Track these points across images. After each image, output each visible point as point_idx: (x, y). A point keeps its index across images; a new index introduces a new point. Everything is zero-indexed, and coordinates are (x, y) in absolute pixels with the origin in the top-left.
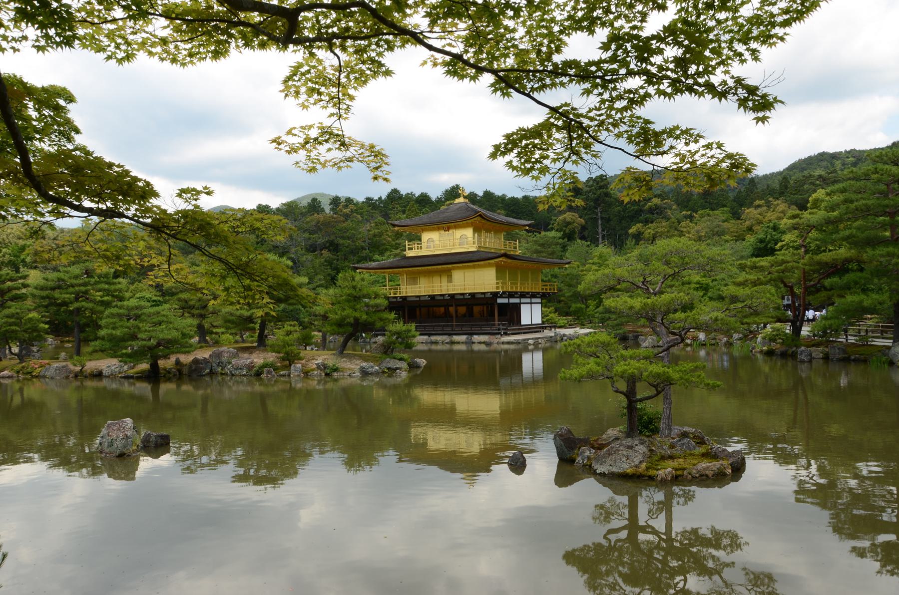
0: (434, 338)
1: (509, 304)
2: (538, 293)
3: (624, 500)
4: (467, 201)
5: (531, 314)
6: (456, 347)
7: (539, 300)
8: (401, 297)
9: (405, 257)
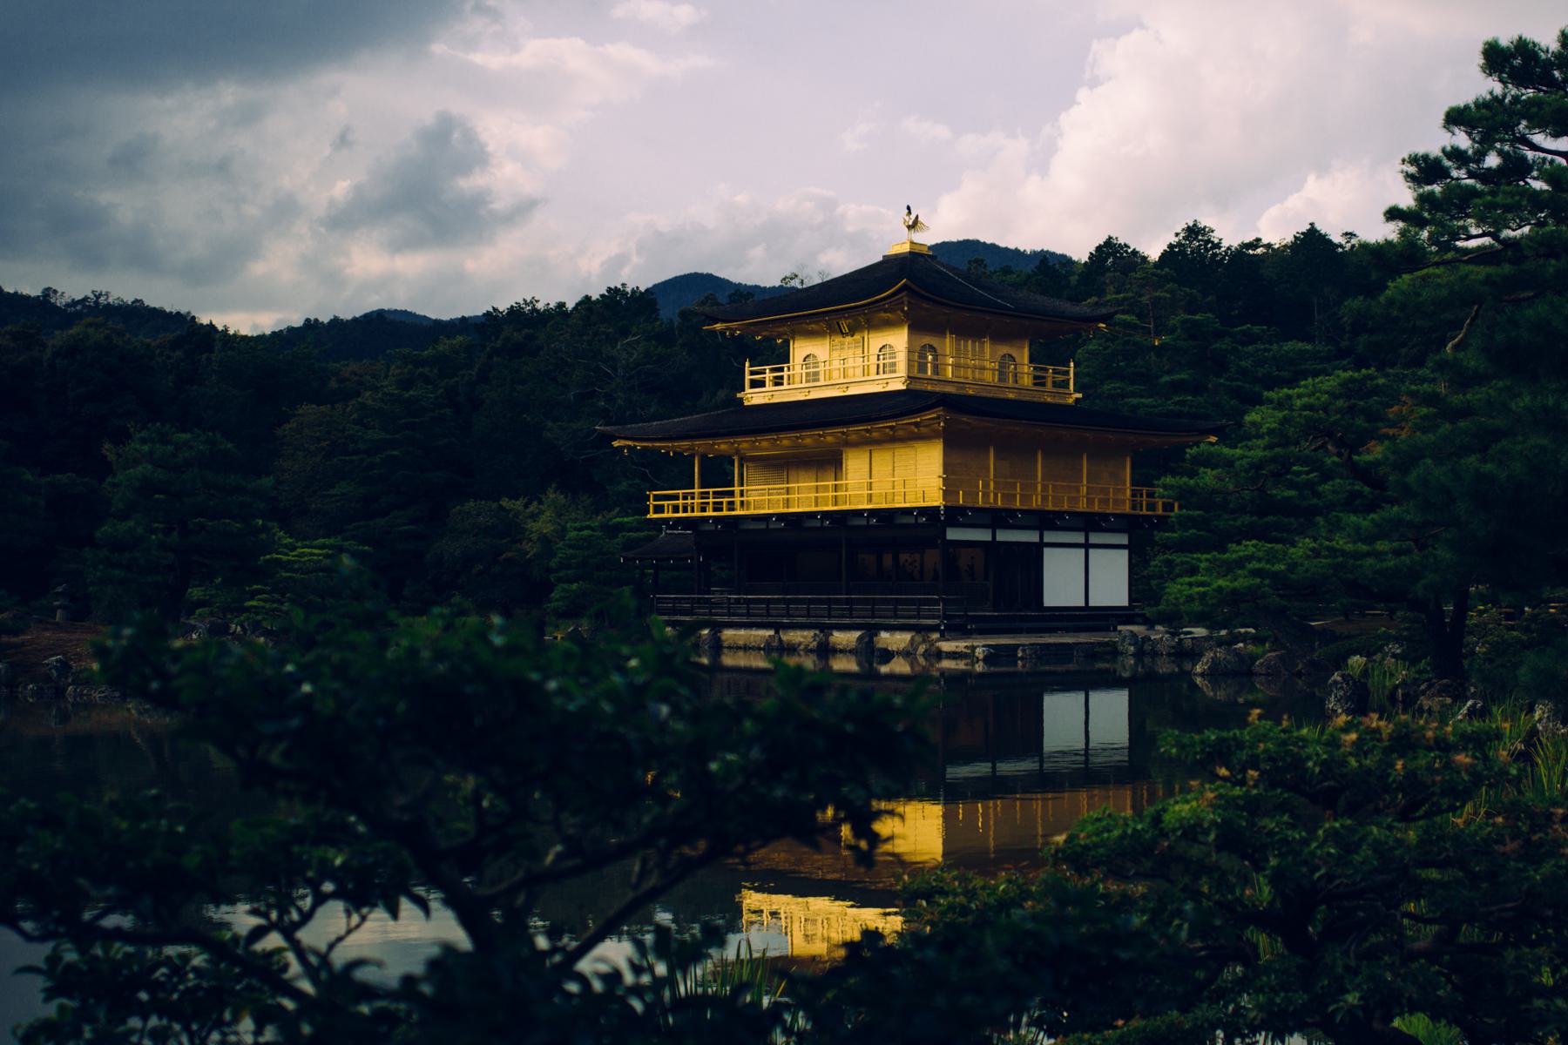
5: (1085, 578)
6: (843, 664)
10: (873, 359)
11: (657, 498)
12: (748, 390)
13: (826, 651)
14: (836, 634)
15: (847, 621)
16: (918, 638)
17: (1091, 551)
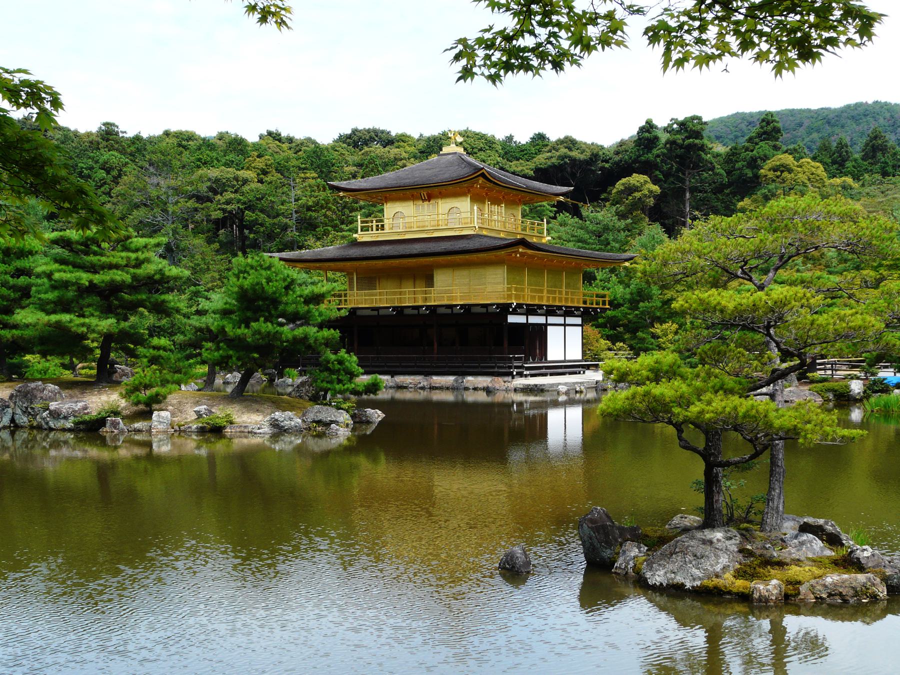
0: (400, 379)
1: (527, 325)
2: (577, 309)
3: (698, 638)
4: (460, 150)
5: (564, 342)
7: (578, 321)
9: (355, 243)
14: (435, 378)
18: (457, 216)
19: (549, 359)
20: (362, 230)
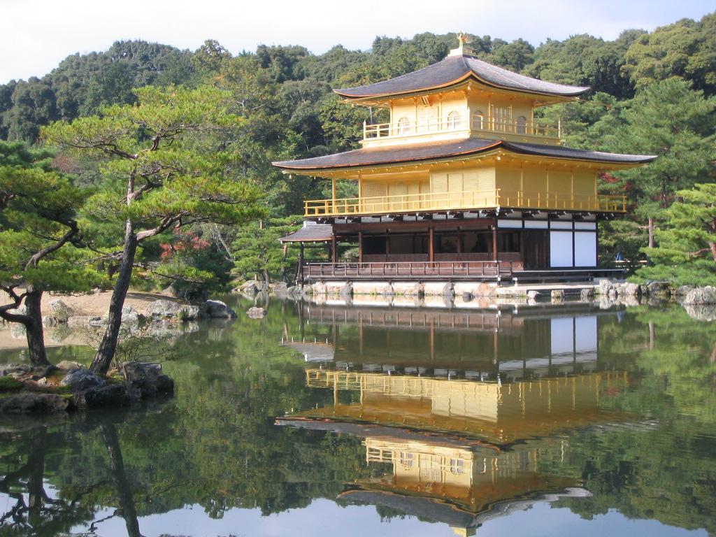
0: (397, 286)
5: (571, 247)
6: (430, 302)
7: (592, 226)
8: (350, 217)
10: (445, 121)
11: (309, 204)
12: (365, 139)
13: (422, 295)
15: (438, 276)
16: (484, 286)
17: (576, 233)
18: (448, 122)
19: (553, 264)
20: (367, 137)
